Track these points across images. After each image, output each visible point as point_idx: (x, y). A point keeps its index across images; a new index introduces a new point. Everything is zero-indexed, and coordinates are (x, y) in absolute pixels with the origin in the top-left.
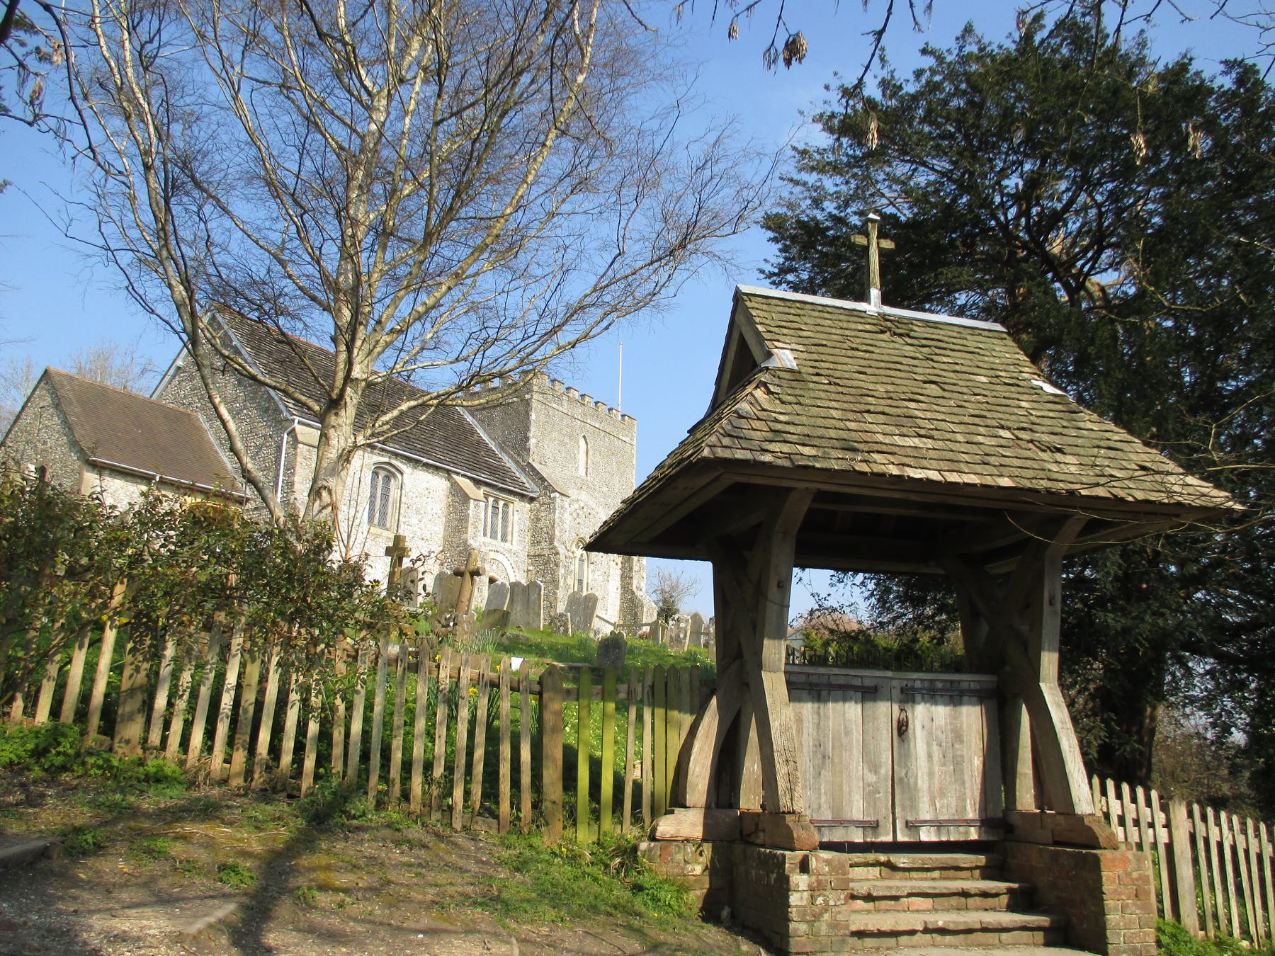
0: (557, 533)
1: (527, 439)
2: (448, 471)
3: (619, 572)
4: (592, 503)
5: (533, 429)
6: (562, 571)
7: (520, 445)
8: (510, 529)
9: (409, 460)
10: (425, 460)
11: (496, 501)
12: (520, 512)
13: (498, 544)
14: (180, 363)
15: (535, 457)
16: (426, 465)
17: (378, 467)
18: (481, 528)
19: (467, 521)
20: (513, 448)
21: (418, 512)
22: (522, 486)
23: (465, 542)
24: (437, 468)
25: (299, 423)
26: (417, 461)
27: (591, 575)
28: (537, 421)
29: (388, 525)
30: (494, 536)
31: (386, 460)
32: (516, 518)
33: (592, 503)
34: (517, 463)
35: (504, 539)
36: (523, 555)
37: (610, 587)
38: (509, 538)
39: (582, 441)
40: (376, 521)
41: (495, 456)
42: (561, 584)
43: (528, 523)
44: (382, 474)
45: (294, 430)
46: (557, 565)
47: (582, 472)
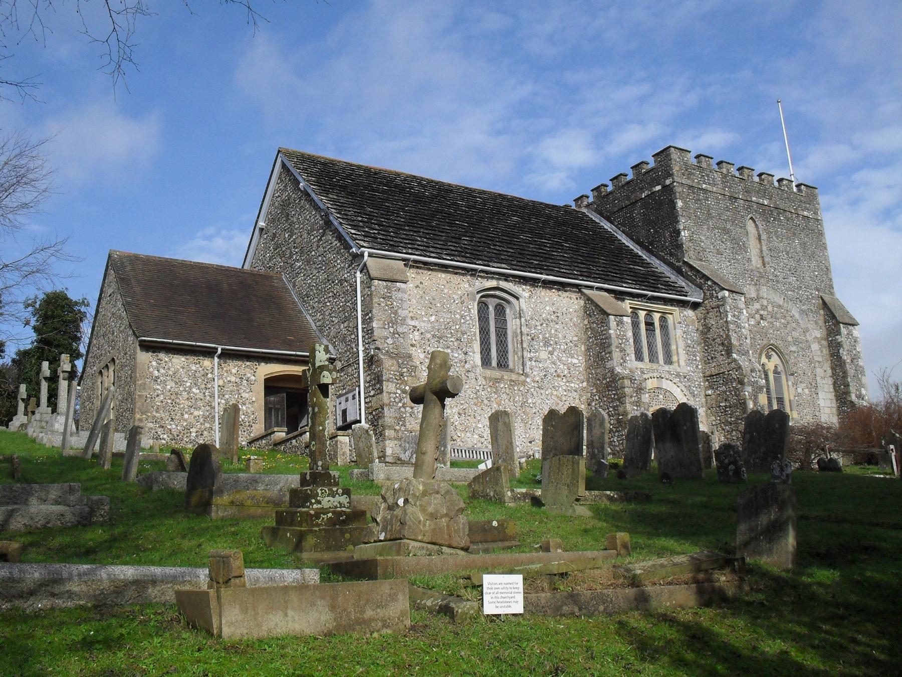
0: (735, 342)
8: (673, 347)
10: (544, 277)
11: (649, 313)
12: (682, 324)
14: (261, 224)
15: (691, 253)
17: (486, 294)
18: (631, 350)
19: (610, 345)
21: (547, 343)
22: (681, 292)
23: (612, 370)
25: (370, 255)
27: (792, 391)
28: (686, 208)
31: (493, 283)
32: (679, 332)
34: (670, 265)
35: (669, 360)
36: (698, 378)
37: (821, 403)
38: (675, 358)
39: (750, 226)
40: (494, 363)
41: (642, 262)
43: (696, 336)
44: (492, 303)
45: (365, 265)
47: (756, 262)
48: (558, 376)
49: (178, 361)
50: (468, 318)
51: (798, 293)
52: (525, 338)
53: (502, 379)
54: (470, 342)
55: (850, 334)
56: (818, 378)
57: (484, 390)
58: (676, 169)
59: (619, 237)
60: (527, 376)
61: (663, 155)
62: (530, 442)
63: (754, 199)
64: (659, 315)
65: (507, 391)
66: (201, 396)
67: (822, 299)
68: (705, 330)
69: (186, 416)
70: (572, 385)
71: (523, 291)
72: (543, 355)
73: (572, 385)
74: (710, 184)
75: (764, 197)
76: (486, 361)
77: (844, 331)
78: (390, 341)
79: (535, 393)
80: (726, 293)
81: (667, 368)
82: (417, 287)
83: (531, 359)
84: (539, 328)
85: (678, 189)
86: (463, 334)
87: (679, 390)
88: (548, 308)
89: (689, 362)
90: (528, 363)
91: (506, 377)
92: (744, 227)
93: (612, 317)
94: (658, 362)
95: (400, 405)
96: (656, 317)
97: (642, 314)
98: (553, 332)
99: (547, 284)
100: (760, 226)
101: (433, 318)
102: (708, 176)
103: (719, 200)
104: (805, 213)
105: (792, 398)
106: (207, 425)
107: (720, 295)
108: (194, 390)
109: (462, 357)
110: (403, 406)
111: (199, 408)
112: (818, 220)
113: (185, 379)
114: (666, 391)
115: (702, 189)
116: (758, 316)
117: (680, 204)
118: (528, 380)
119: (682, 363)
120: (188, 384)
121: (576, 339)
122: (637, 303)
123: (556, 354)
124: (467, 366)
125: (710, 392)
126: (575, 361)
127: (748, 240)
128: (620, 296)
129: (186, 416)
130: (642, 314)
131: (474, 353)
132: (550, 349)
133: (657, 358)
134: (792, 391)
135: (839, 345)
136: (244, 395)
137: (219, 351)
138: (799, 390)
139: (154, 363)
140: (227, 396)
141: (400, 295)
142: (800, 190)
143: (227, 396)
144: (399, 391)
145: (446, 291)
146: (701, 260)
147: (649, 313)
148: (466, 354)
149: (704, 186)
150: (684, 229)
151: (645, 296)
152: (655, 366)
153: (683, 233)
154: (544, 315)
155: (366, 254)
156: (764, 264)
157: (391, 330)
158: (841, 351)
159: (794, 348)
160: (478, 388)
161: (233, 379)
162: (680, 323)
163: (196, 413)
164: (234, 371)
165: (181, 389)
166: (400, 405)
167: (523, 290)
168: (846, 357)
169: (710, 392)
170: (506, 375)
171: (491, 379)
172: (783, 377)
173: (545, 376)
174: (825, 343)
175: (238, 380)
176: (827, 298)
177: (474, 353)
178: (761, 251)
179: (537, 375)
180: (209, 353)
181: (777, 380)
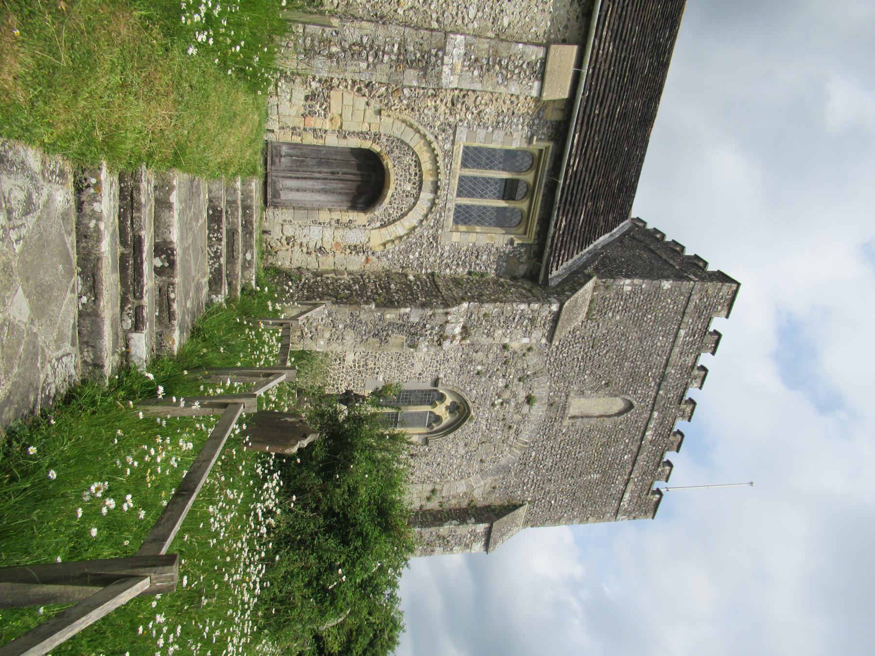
0: (488, 308)
1: (627, 276)
4: (524, 437)
5: (646, 285)
6: (414, 315)
13: (452, 199)
30: (467, 187)
33: (524, 437)
39: (618, 404)
42: (390, 315)
46: (423, 306)
47: (577, 405)
51: (532, 467)
56: (419, 487)
61: (722, 277)
63: (656, 414)
64: (531, 181)
67: (521, 505)
77: (481, 528)
80: (555, 308)
81: (451, 206)
85: (686, 285)
89: (456, 249)
94: (458, 195)
96: (524, 205)
97: (529, 177)
100: (621, 418)
102: (693, 343)
104: (627, 496)
107: (553, 300)
114: (417, 198)
115: (679, 328)
116: (507, 395)
117: (666, 285)
119: (456, 237)
122: (547, 164)
126: (472, 12)
130: (529, 177)
133: (466, 196)
135: (463, 521)
142: (654, 493)
149: (682, 332)
150: (632, 285)
152: (455, 183)
153: (628, 281)
156: (573, 417)
158: (454, 522)
168: (444, 530)
169: (411, 278)
174: (464, 505)
176: (522, 512)
178: (588, 417)
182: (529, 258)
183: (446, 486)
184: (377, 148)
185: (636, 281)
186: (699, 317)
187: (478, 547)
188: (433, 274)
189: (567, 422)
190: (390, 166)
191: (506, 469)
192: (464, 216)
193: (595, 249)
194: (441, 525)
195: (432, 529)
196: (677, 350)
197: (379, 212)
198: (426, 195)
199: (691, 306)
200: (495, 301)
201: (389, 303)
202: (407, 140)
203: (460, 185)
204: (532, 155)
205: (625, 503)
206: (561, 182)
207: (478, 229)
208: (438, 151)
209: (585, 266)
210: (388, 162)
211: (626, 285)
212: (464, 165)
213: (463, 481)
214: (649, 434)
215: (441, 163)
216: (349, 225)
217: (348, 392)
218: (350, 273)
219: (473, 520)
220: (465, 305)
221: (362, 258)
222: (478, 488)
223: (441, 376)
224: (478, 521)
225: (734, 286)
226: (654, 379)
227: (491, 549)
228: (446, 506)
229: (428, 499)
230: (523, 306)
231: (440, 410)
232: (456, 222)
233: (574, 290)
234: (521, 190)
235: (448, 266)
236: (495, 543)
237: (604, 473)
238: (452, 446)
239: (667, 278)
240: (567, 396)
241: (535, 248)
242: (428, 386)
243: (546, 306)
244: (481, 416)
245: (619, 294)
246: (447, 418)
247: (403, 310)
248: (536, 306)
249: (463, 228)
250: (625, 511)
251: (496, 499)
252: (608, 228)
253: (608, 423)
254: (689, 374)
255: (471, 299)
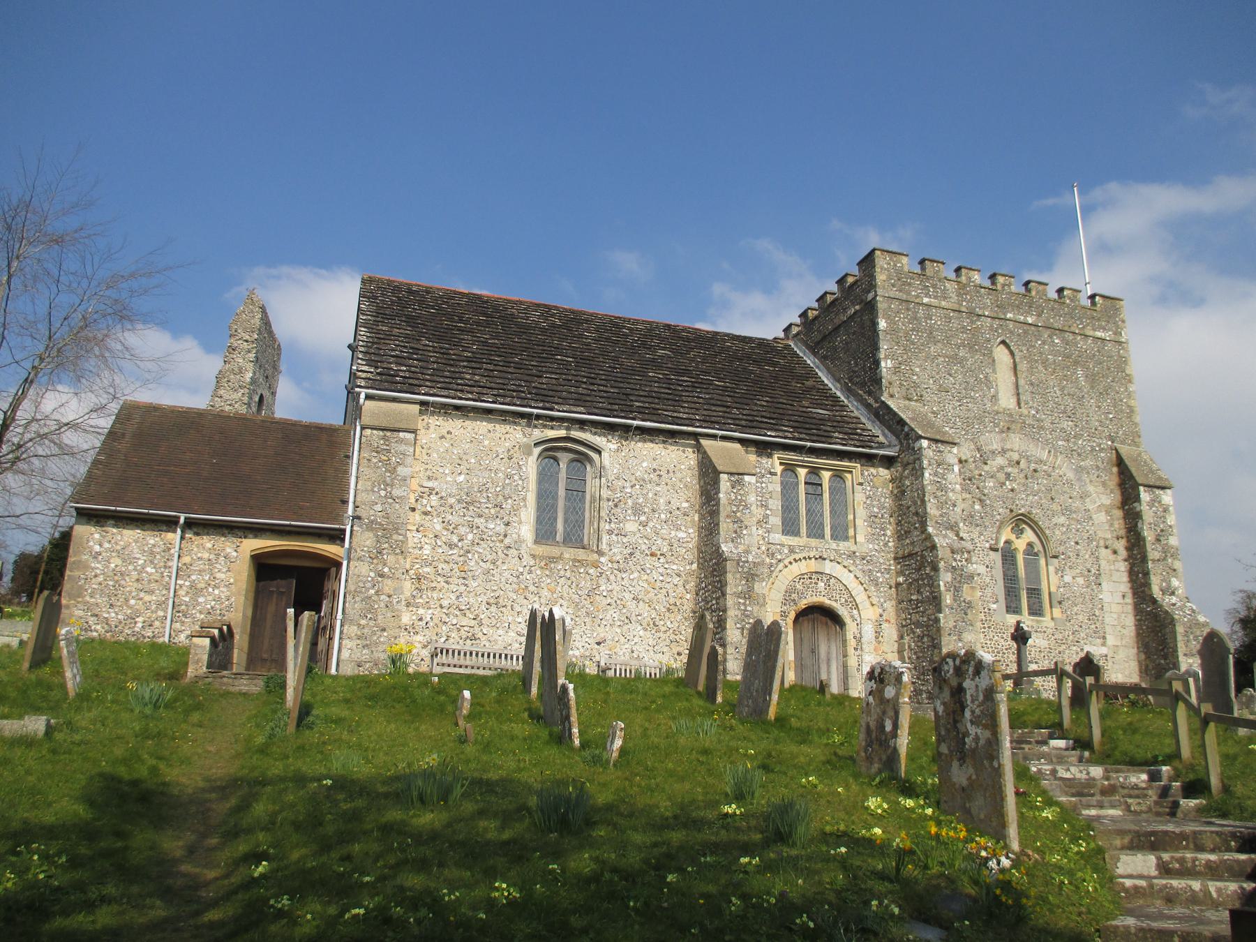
1: (877, 363)
2: (695, 436)
3: (1123, 567)
5: (884, 346)
6: (945, 578)
7: (866, 379)
9: (611, 428)
10: (635, 423)
11: (814, 471)
12: (868, 490)
13: (829, 545)
15: (895, 390)
16: (642, 431)
20: (862, 385)
21: (637, 510)
22: (870, 441)
24: (672, 434)
25: (368, 397)
26: (627, 428)
27: (1054, 579)
28: (893, 331)
29: (586, 541)
30: (816, 531)
37: (1105, 596)
39: (1001, 354)
40: (559, 537)
42: (948, 599)
43: (888, 502)
44: (564, 458)
46: (935, 569)
47: (1007, 401)
48: (652, 555)
49: (130, 536)
50: (516, 477)
51: (1075, 443)
52: (604, 504)
53: (561, 558)
54: (515, 510)
55: (1155, 501)
56: (1103, 563)
57: (530, 572)
58: (880, 278)
59: (820, 374)
60: (600, 553)
62: (599, 644)
63: (1009, 315)
65: (568, 574)
66: (157, 576)
68: (899, 495)
69: (132, 602)
70: (675, 567)
71: (607, 444)
72: (631, 526)
73: (675, 567)
74: (936, 297)
75: (1029, 313)
76: (544, 533)
77: (1145, 495)
78: (378, 507)
79: (612, 578)
80: (925, 443)
82: (442, 437)
83: (610, 532)
84: (629, 490)
86: (506, 499)
87: (852, 575)
88: (645, 464)
89: (872, 538)
90: (605, 538)
91: (566, 556)
92: (990, 354)
93: (724, 477)
94: (823, 537)
95: (372, 592)
96: (826, 475)
97: (802, 472)
98: (650, 495)
99: (642, 431)
100: (1016, 352)
101: (461, 478)
102: (934, 286)
103: (950, 318)
104: (1099, 334)
105: (1053, 589)
106: (161, 613)
107: (917, 445)
108: (148, 569)
109: (501, 528)
110: (377, 593)
111: (151, 592)
112: (1120, 343)
113: (138, 556)
116: (1001, 476)
117: (882, 324)
118: (603, 559)
119: (860, 538)
120: (141, 562)
121: (685, 505)
122: (792, 456)
123: (651, 524)
124: (507, 541)
125: (901, 579)
126: (681, 535)
127: (994, 371)
128: (764, 448)
129: (132, 602)
130: (802, 472)
131: (520, 523)
132: (643, 518)
133: (823, 530)
134: (1054, 579)
136: (219, 575)
137: (182, 521)
138: (1067, 579)
139: (97, 536)
140: (193, 577)
141: (402, 448)
142: (1094, 303)
143: (193, 577)
144: (372, 574)
145: (486, 442)
146: (910, 400)
147: (814, 471)
148: (507, 524)
149: (926, 300)
150: (886, 358)
151: (803, 447)
152: (814, 542)
153: (883, 364)
154: (638, 474)
155: (363, 396)
157: (383, 493)
158: (1139, 525)
159: (1062, 520)
160: (521, 570)
161: (206, 555)
162: (861, 484)
163: (147, 598)
164: (209, 545)
165: (131, 567)
166: (372, 592)
167: (608, 441)
168: (1148, 535)
169: (901, 579)
170: (569, 553)
171: (542, 558)
172: (1042, 562)
173: (631, 554)
174: (1119, 513)
175: (212, 557)
176: (1124, 450)
177: (520, 523)
178: (1017, 387)
179: (618, 552)
180: (171, 524)
181: (1033, 568)
182: (873, 466)
183: (1100, 534)
184: (792, 615)
185: (882, 356)
186: (910, 284)
187: (1167, 498)
188: (895, 559)
189: (1024, 411)
190: (805, 601)
191: (1079, 470)
192: (840, 533)
193: (841, 390)
194: (1144, 539)
195: (1149, 549)
196: (943, 303)
197: (843, 612)
198: (828, 567)
199: (898, 295)
200: (923, 501)
201: (936, 601)
202: (784, 588)
203: (815, 536)
204: (784, 470)
205: (1107, 335)
206: (809, 444)
207: (851, 517)
208: (791, 559)
209: (868, 406)
210: (803, 604)
211: (886, 365)
212: (797, 533)
213: (1094, 516)
214: (1030, 320)
215: (801, 556)
216: (859, 640)
217: (1014, 638)
218: (902, 637)
219: (1136, 505)
220: (930, 529)
221: (885, 625)
222: (1101, 499)
223: (987, 545)
224: (1137, 499)
225: (878, 253)
226: (972, 322)
227: (1166, 484)
228: (1123, 532)
229: (1115, 552)
230: (927, 475)
231: (1020, 545)
232: (846, 538)
233: (902, 422)
234: (814, 479)
235: (886, 545)
236: (1160, 478)
237: (1076, 363)
238: (1057, 526)
239: (874, 324)
240: (998, 413)
241: (863, 461)
242: (997, 557)
243: (924, 452)
244: (1024, 504)
245: (896, 370)
246: (1029, 536)
247: (942, 588)
248: (925, 462)
249: (851, 532)
250: (1115, 334)
251: (1112, 478)
252: (810, 374)
253: (1023, 366)
254: (965, 286)
255: (924, 525)
